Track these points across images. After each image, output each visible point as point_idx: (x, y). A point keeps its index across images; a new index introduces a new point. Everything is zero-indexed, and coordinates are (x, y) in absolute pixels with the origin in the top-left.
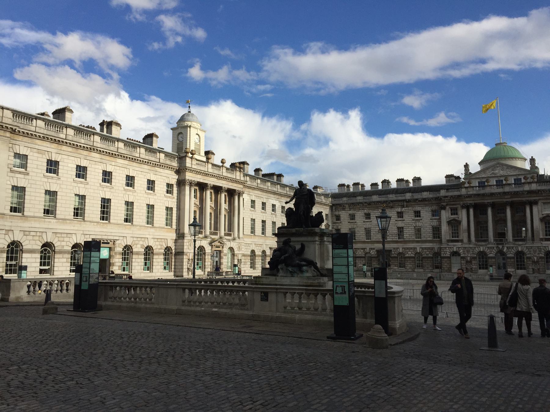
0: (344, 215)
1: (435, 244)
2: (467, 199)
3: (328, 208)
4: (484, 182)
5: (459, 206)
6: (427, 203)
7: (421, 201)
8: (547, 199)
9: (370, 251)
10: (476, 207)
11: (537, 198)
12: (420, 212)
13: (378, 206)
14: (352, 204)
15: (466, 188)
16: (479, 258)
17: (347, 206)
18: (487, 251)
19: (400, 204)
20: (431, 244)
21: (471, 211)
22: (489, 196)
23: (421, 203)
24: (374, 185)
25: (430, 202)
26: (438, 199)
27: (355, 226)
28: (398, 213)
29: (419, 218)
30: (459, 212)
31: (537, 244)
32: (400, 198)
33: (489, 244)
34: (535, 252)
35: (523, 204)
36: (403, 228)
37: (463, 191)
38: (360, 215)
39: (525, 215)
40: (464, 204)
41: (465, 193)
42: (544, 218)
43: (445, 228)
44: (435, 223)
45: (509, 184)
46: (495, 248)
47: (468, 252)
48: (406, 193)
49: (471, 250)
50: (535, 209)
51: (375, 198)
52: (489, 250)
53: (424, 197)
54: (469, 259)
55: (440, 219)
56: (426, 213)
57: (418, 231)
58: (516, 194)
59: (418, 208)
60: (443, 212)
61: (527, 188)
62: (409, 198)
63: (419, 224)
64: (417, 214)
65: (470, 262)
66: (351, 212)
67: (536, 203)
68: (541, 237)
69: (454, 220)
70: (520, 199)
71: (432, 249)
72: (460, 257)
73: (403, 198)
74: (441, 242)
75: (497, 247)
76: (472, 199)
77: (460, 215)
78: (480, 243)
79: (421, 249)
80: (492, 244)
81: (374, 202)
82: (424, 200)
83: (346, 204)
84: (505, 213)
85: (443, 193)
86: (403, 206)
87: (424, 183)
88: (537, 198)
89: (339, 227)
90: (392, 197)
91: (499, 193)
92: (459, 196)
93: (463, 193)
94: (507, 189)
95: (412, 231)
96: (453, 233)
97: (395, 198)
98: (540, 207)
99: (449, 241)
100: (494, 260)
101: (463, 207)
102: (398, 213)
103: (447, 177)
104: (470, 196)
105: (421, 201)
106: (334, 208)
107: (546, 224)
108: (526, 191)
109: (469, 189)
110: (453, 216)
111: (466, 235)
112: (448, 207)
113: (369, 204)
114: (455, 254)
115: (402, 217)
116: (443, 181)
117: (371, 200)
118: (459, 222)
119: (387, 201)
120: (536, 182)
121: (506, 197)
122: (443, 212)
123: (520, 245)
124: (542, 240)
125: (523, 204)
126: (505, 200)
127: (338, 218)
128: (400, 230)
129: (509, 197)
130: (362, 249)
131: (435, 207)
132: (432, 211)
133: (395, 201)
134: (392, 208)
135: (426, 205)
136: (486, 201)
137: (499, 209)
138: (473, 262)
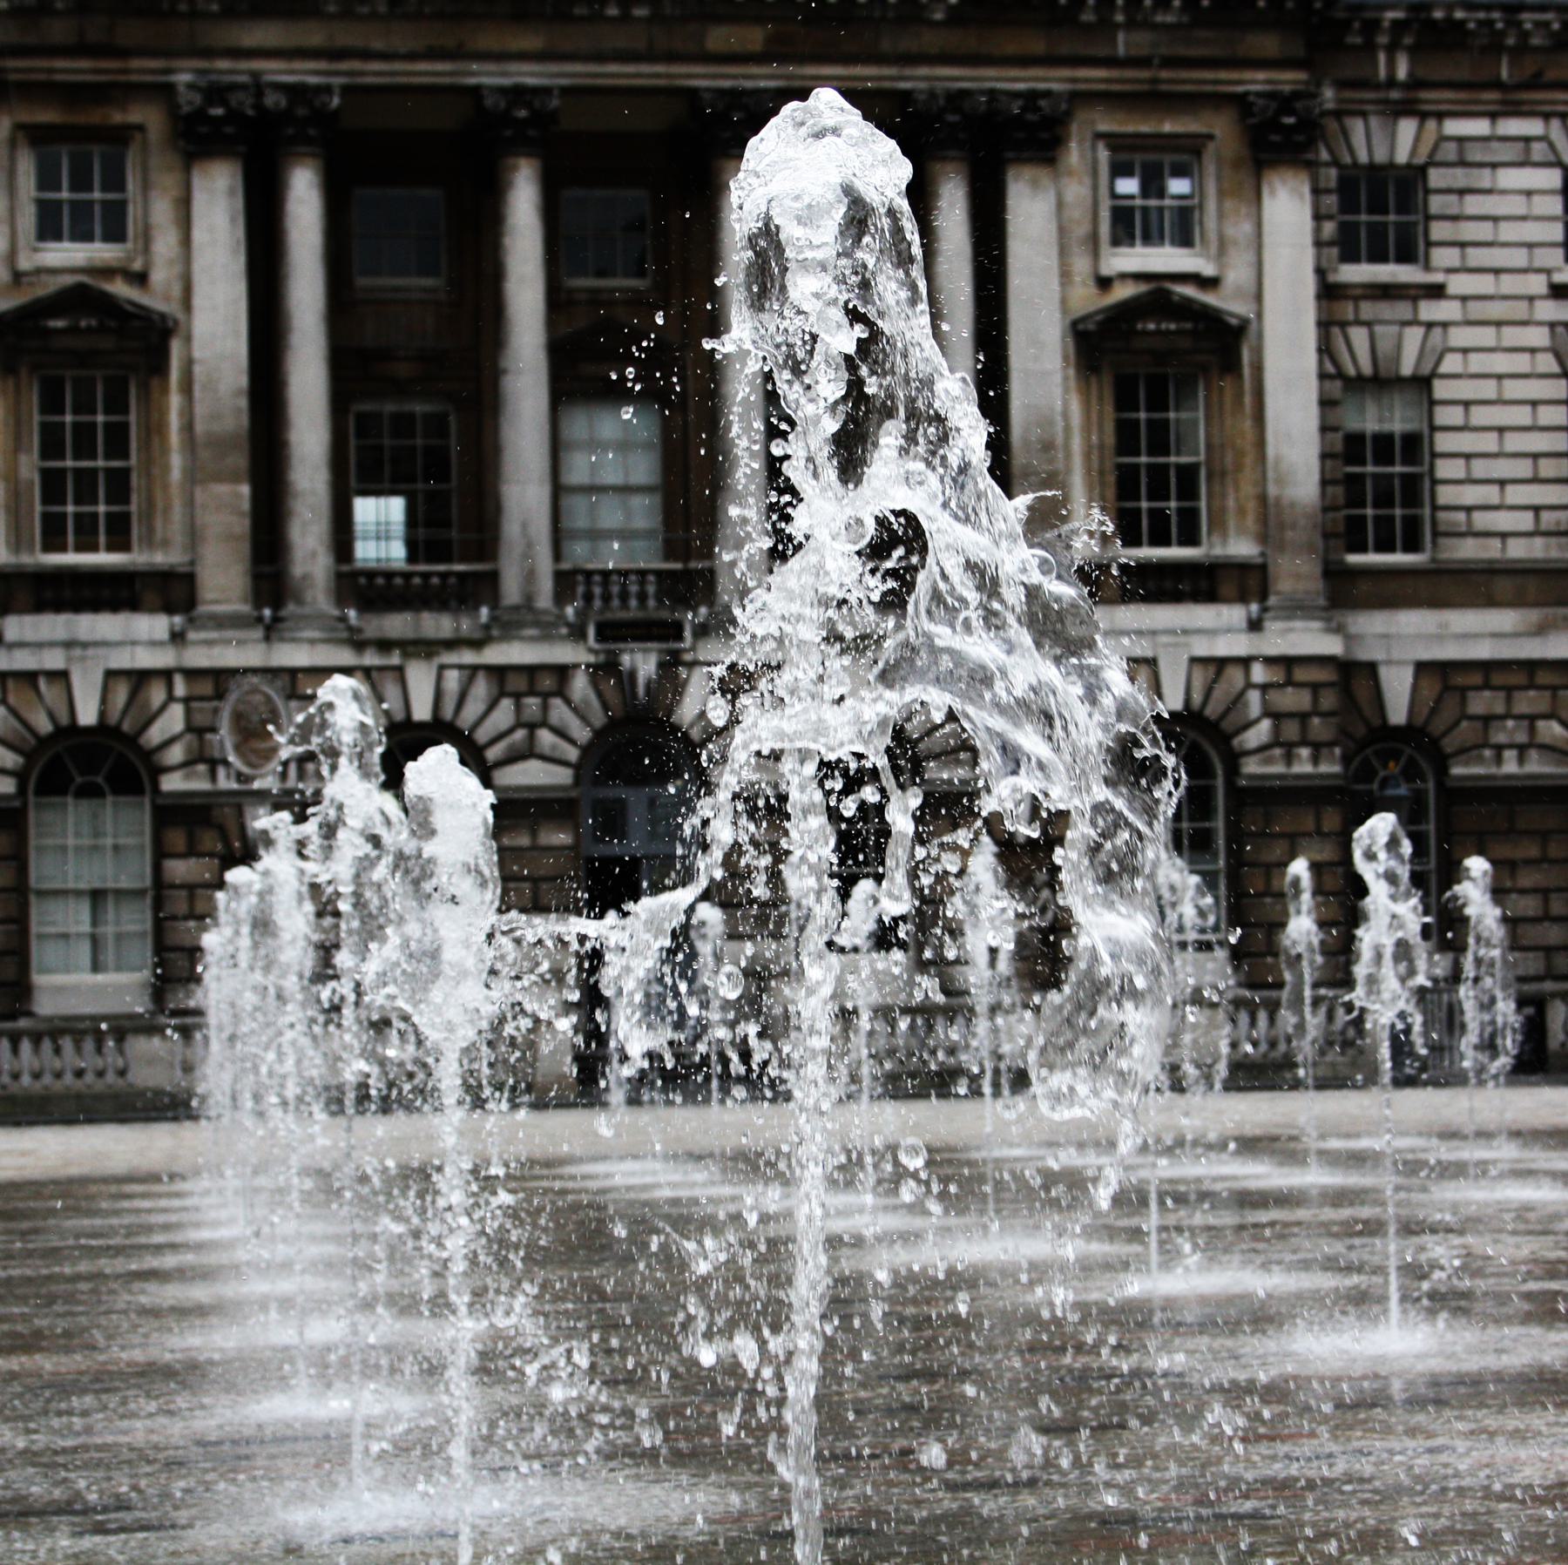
5: (148, 116)
11: (1055, 80)
33: (506, 626)
40: (216, 92)
46: (580, 685)
52: (504, 713)
75: (606, 669)
77: (165, 244)
78: (396, 624)
80: (547, 630)
88: (1055, 80)
96: (52, 485)
98: (1076, 190)
101: (197, 140)
107: (1125, 400)
110: (68, 255)
121: (719, 38)
129: (753, 37)
136: (487, 76)
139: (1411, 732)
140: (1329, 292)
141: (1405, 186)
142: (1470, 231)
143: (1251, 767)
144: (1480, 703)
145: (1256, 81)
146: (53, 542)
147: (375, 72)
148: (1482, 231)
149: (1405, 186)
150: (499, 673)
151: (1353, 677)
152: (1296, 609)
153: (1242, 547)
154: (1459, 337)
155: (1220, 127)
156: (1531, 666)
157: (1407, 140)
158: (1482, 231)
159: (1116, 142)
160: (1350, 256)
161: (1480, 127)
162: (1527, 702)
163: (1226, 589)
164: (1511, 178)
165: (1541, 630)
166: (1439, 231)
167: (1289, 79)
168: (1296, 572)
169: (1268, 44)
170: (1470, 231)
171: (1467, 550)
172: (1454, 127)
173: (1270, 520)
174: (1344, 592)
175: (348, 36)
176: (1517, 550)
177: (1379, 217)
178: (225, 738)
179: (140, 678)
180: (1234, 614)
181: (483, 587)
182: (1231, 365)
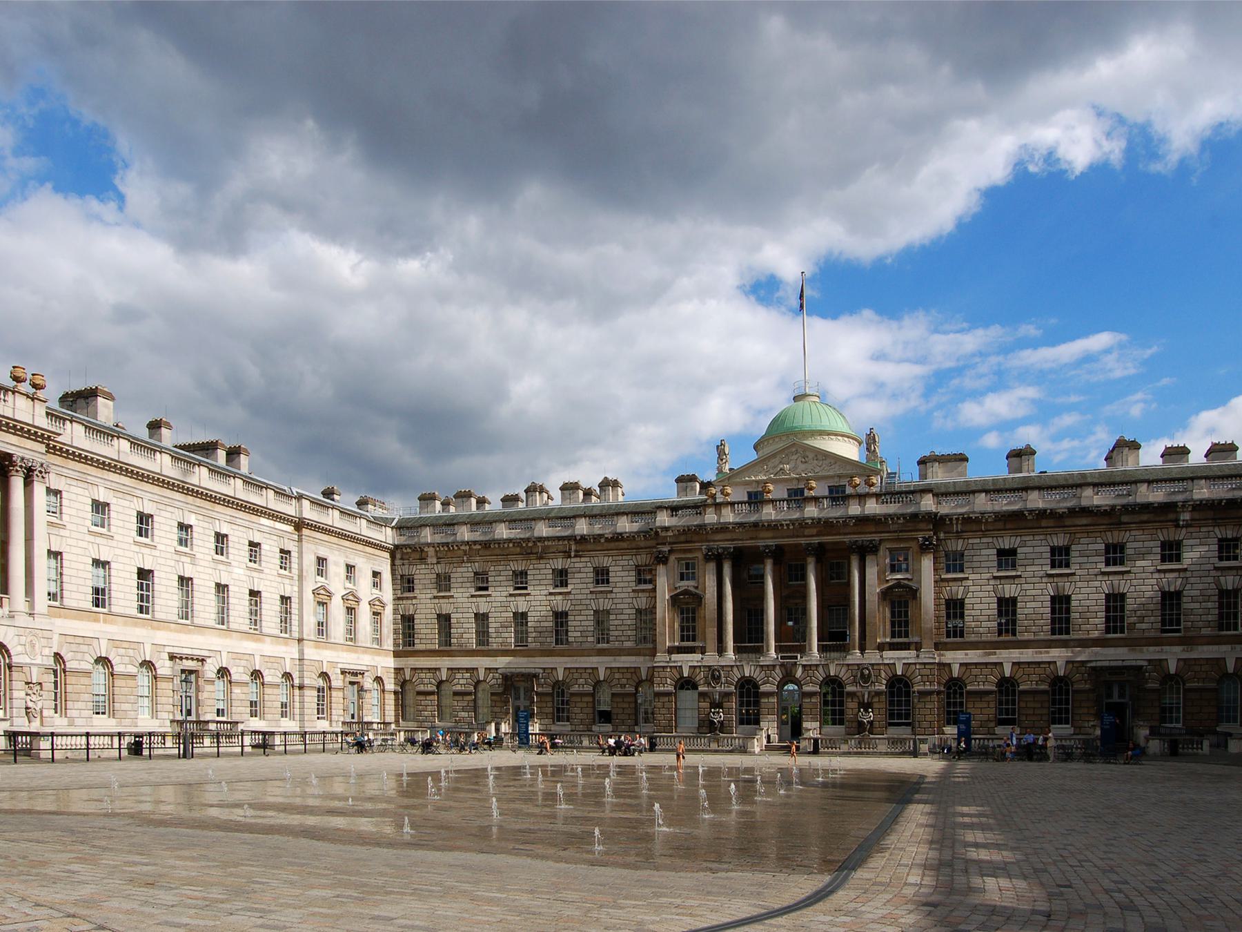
0: (423, 575)
1: (641, 658)
2: (719, 537)
3: (387, 555)
4: (762, 493)
6: (624, 545)
8: (899, 540)
9: (486, 676)
11: (876, 537)
14: (443, 544)
16: (741, 696)
17: (431, 551)
18: (758, 675)
19: (561, 548)
20: (633, 658)
23: (612, 545)
26: (653, 535)
31: (872, 657)
37: (710, 517)
39: (849, 585)
43: (663, 611)
44: (642, 602)
45: (816, 499)
55: (654, 590)
57: (601, 617)
58: (825, 525)
59: (606, 562)
60: (661, 569)
61: (854, 509)
63: (604, 604)
64: (602, 576)
69: (686, 592)
71: (636, 670)
72: (695, 694)
74: (653, 653)
76: (728, 536)
79: (608, 672)
81: (499, 542)
82: (618, 537)
83: (429, 545)
84: (804, 577)
85: (663, 519)
86: (567, 555)
88: (876, 537)
90: (543, 530)
91: (793, 522)
94: (811, 511)
95: (589, 623)
99: (672, 650)
101: (707, 559)
104: (723, 528)
106: (398, 556)
111: (712, 632)
112: (672, 558)
113: (486, 545)
114: (686, 684)
118: (698, 599)
120: (877, 496)
121: (807, 532)
122: (661, 569)
124: (881, 647)
128: (560, 617)
129: (814, 531)
130: (467, 670)
131: (643, 559)
132: (639, 570)
133: (548, 539)
134: (541, 558)
135: (622, 552)
136: (761, 543)
139: (958, 679)
142: (975, 565)
143: (916, 688)
144: (975, 671)
146: (682, 640)
147: (740, 544)
148: (978, 564)
153: (916, 639)
154: (972, 589)
156: (986, 664)
158: (978, 564)
159: (891, 550)
160: (948, 571)
161: (978, 541)
162: (986, 671)
163: (913, 647)
164: (983, 552)
165: (990, 654)
166: (966, 565)
169: (922, 526)
170: (975, 565)
171: (973, 638)
172: (970, 541)
179: (695, 667)
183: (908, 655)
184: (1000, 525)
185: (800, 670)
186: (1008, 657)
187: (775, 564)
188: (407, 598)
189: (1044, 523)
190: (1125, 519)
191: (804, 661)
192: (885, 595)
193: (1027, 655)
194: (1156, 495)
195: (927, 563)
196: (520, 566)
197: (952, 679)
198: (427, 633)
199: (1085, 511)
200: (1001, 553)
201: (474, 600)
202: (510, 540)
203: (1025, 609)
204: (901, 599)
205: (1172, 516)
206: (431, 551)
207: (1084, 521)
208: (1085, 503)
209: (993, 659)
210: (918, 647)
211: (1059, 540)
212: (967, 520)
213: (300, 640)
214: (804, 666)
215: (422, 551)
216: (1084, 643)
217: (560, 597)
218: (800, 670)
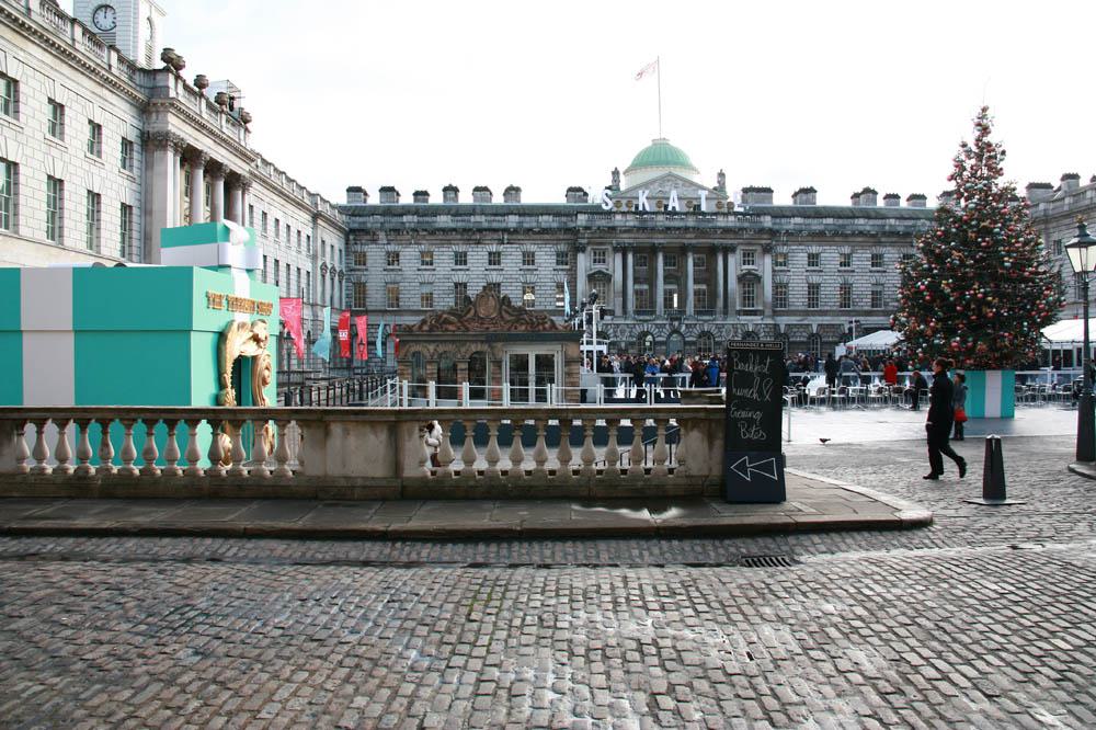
0: (375, 254)
2: (622, 236)
7: (539, 233)
10: (637, 250)
11: (736, 242)
12: (533, 254)
13: (450, 237)
15: (623, 213)
17: (382, 235)
21: (630, 257)
22: (661, 232)
23: (538, 237)
24: (421, 195)
25: (555, 237)
26: (574, 231)
27: (399, 278)
28: (490, 254)
29: (531, 267)
30: (609, 259)
32: (495, 225)
33: (657, 318)
34: (728, 333)
35: (712, 251)
36: (499, 284)
38: (410, 254)
40: (618, 244)
41: (622, 224)
42: (744, 275)
46: (667, 327)
47: (623, 332)
48: (508, 214)
49: (628, 330)
50: (732, 260)
51: (443, 221)
53: (544, 225)
54: (623, 345)
56: (545, 257)
59: (533, 248)
60: (581, 257)
62: (514, 225)
64: (529, 258)
65: (626, 350)
66: (391, 248)
67: (732, 249)
68: (738, 308)
69: (600, 272)
70: (709, 241)
73: (503, 225)
76: (633, 236)
77: (611, 264)
78: (641, 318)
82: (544, 231)
86: (501, 242)
87: (527, 198)
88: (736, 242)
89: (363, 279)
91: (679, 229)
92: (613, 229)
93: (617, 224)
97: (486, 225)
98: (738, 257)
100: (664, 347)
101: (616, 250)
102: (490, 254)
103: (570, 190)
104: (629, 230)
105: (539, 233)
106: (351, 237)
108: (720, 228)
109: (629, 217)
112: (589, 248)
115: (499, 264)
116: (558, 198)
117: (437, 225)
119: (470, 230)
121: (688, 236)
122: (581, 257)
123: (705, 321)
124: (739, 313)
125: (712, 251)
126: (686, 241)
127: (361, 259)
129: (693, 236)
131: (562, 247)
132: (558, 255)
134: (479, 243)
135: (546, 242)
137: (676, 255)
138: (631, 351)
140: (774, 271)
141: (785, 256)
144: (795, 330)
145: (763, 242)
147: (641, 240)
149: (785, 256)
150: (656, 325)
151: (776, 326)
152: (769, 317)
153: (760, 308)
155: (759, 248)
156: (802, 325)
157: (785, 249)
162: (801, 330)
167: (769, 241)
168: (768, 312)
169: (765, 237)
171: (793, 308)
173: (764, 304)
174: (775, 314)
175: (637, 236)
176: (800, 308)
177: (781, 262)
178: (619, 334)
180: (759, 318)
181: (653, 313)
182: (759, 281)
183: (757, 319)
184: (810, 238)
185: (684, 328)
186: (815, 322)
187: (665, 258)
188: (359, 270)
189: (837, 239)
190: (883, 239)
191: (686, 322)
192: (741, 279)
193: (827, 320)
194: (900, 226)
195: (768, 260)
196: (461, 248)
197: (781, 335)
198: (376, 298)
199: (861, 233)
200: (811, 256)
201: (420, 273)
202: (454, 230)
203: (823, 292)
204: (750, 280)
205: (909, 240)
206: (382, 235)
207: (860, 239)
208: (861, 228)
209: (806, 322)
210: (760, 313)
211: (847, 250)
212: (787, 233)
213: (312, 305)
214: (687, 325)
215: (374, 234)
216: (859, 313)
217: (495, 273)
218: (684, 328)
